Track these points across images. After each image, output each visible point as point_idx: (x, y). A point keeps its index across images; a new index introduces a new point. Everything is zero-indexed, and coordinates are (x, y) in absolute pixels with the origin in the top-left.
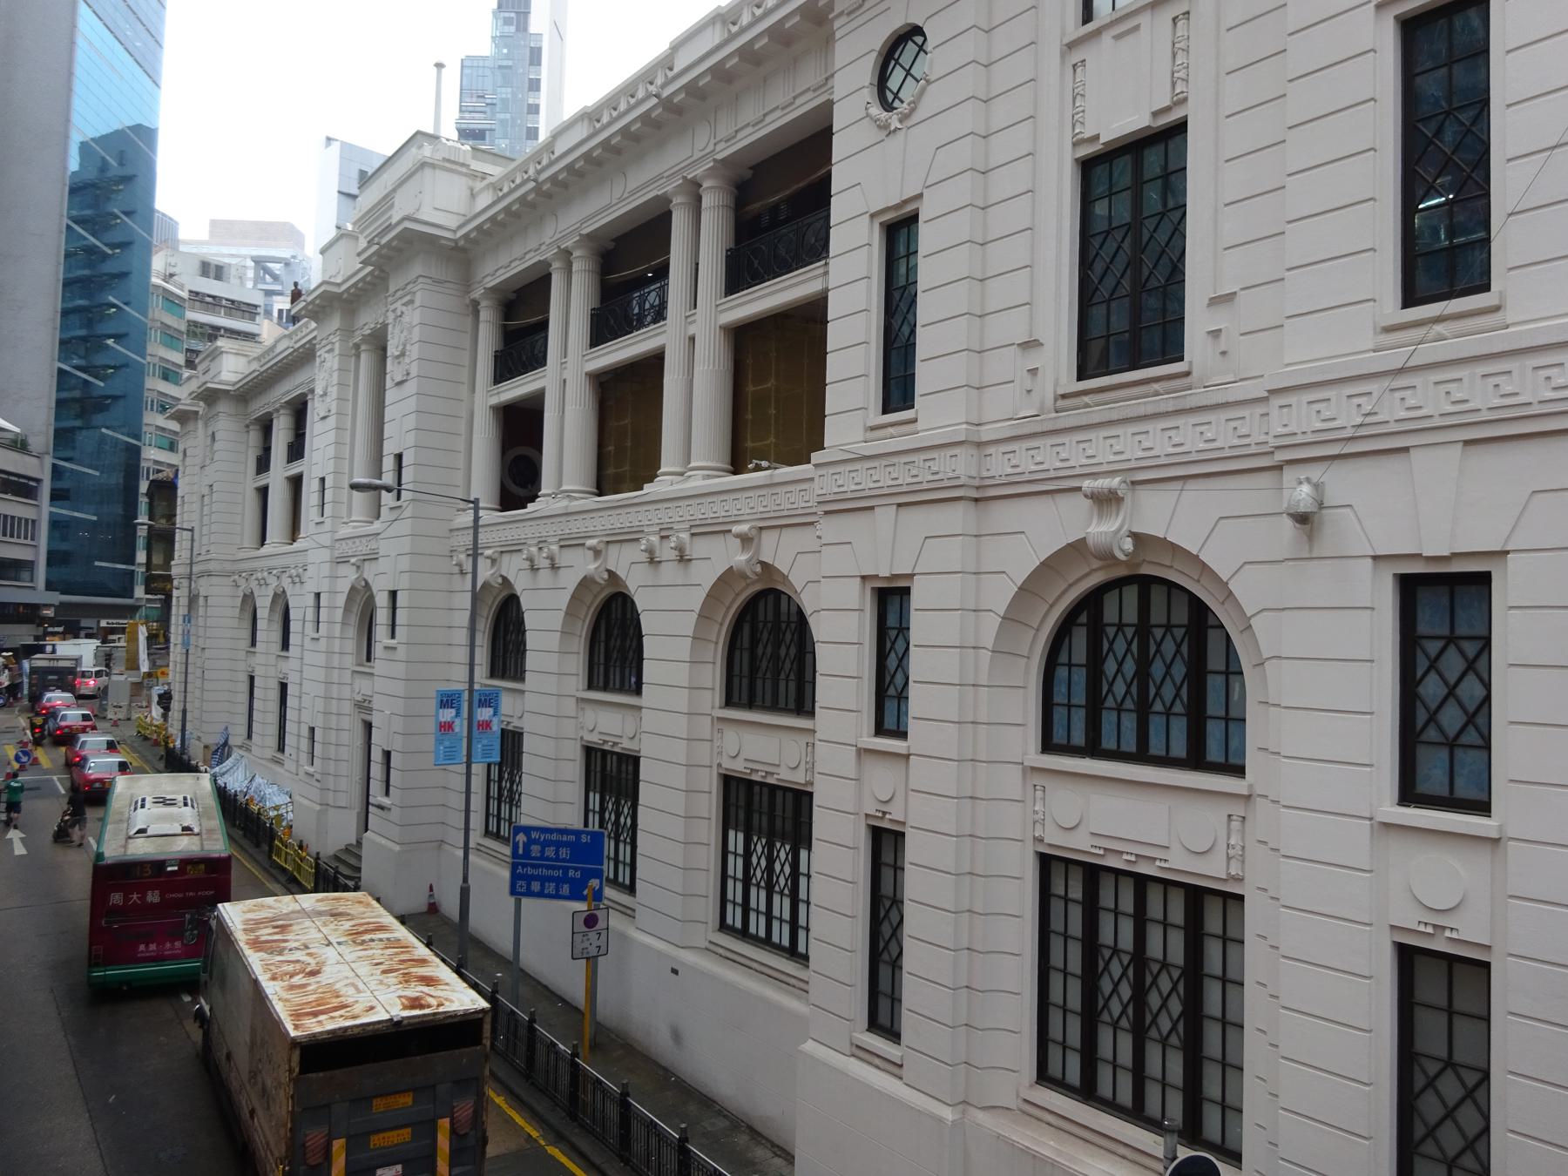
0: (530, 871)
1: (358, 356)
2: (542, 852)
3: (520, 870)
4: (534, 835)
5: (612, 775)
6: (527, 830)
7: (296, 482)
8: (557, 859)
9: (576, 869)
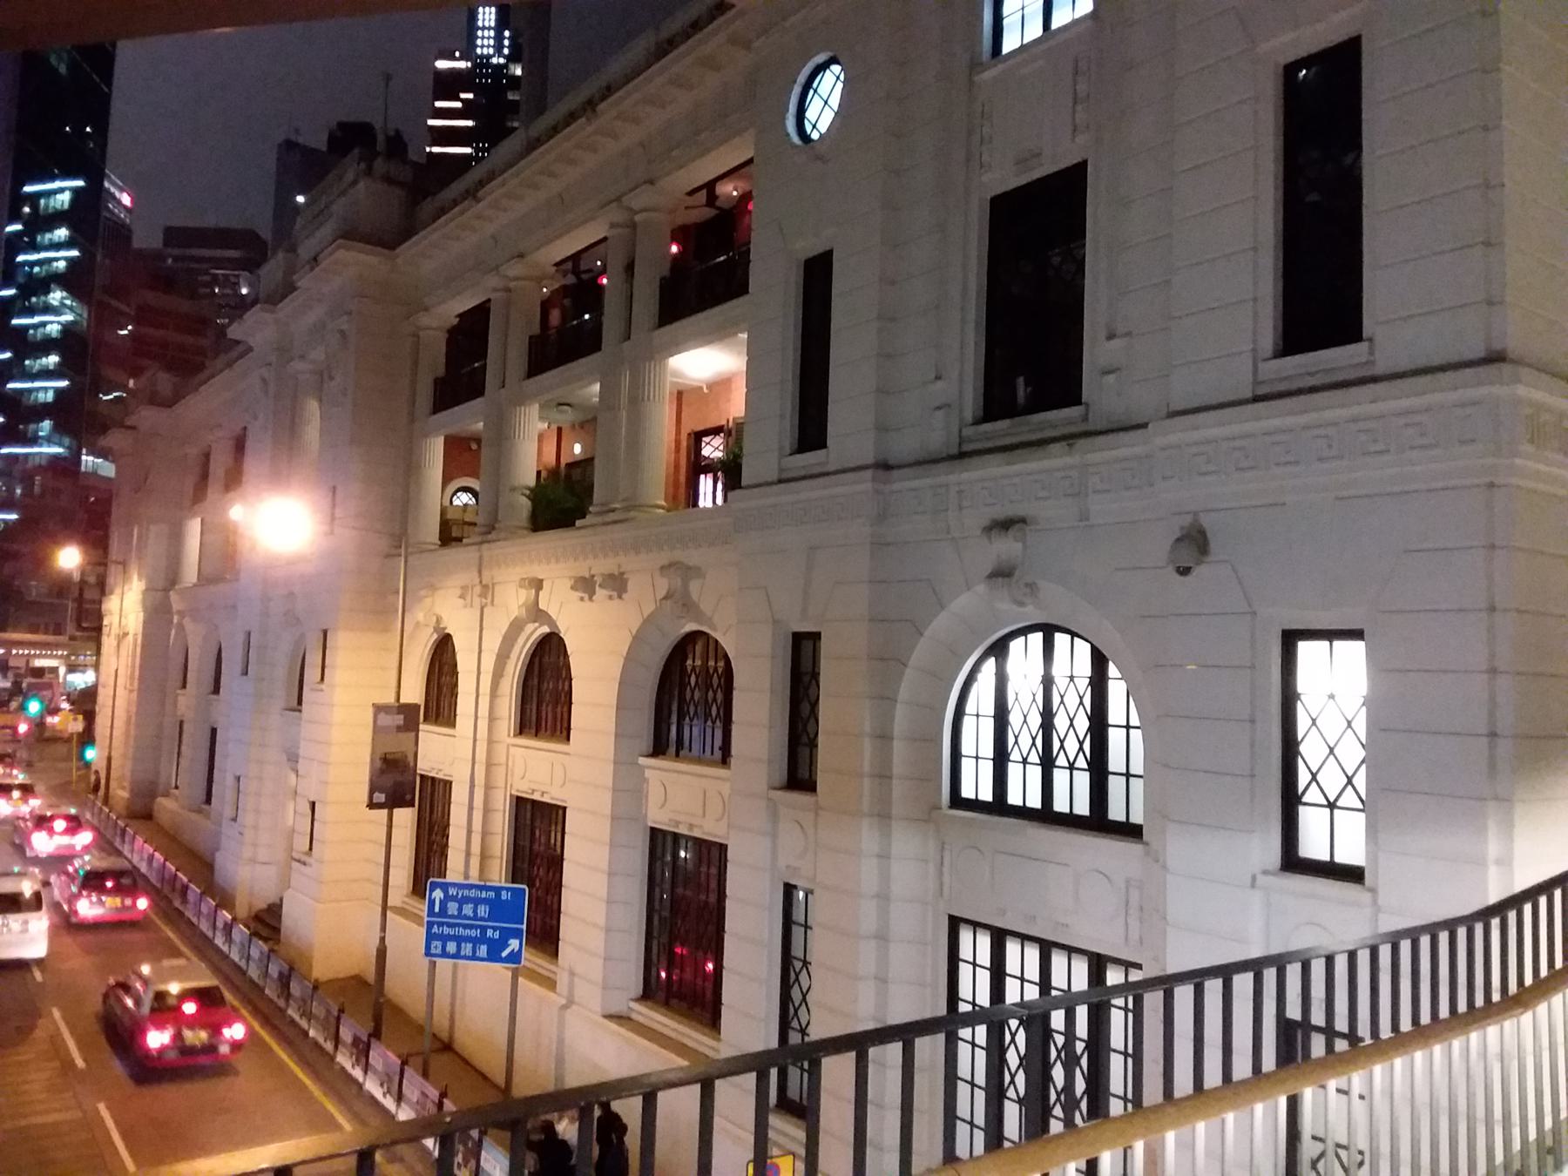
0: (446, 930)
2: (460, 909)
3: (435, 929)
4: (452, 891)
5: (537, 830)
8: (475, 918)
9: (494, 928)
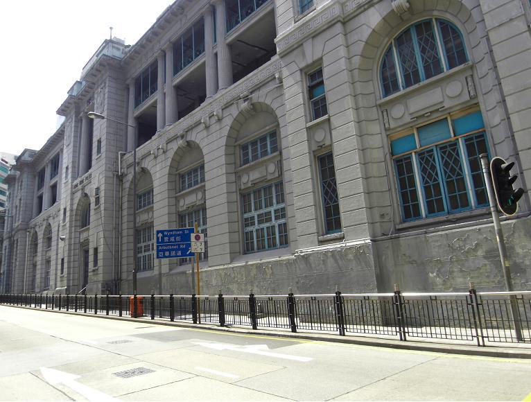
1: (82, 123)
6: (162, 232)
7: (54, 187)
